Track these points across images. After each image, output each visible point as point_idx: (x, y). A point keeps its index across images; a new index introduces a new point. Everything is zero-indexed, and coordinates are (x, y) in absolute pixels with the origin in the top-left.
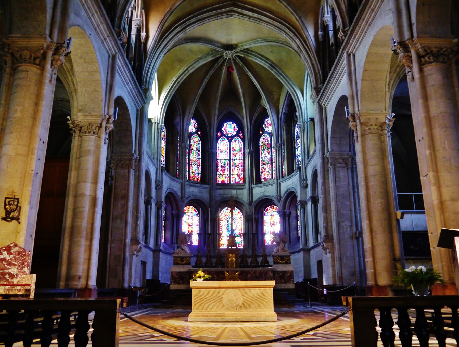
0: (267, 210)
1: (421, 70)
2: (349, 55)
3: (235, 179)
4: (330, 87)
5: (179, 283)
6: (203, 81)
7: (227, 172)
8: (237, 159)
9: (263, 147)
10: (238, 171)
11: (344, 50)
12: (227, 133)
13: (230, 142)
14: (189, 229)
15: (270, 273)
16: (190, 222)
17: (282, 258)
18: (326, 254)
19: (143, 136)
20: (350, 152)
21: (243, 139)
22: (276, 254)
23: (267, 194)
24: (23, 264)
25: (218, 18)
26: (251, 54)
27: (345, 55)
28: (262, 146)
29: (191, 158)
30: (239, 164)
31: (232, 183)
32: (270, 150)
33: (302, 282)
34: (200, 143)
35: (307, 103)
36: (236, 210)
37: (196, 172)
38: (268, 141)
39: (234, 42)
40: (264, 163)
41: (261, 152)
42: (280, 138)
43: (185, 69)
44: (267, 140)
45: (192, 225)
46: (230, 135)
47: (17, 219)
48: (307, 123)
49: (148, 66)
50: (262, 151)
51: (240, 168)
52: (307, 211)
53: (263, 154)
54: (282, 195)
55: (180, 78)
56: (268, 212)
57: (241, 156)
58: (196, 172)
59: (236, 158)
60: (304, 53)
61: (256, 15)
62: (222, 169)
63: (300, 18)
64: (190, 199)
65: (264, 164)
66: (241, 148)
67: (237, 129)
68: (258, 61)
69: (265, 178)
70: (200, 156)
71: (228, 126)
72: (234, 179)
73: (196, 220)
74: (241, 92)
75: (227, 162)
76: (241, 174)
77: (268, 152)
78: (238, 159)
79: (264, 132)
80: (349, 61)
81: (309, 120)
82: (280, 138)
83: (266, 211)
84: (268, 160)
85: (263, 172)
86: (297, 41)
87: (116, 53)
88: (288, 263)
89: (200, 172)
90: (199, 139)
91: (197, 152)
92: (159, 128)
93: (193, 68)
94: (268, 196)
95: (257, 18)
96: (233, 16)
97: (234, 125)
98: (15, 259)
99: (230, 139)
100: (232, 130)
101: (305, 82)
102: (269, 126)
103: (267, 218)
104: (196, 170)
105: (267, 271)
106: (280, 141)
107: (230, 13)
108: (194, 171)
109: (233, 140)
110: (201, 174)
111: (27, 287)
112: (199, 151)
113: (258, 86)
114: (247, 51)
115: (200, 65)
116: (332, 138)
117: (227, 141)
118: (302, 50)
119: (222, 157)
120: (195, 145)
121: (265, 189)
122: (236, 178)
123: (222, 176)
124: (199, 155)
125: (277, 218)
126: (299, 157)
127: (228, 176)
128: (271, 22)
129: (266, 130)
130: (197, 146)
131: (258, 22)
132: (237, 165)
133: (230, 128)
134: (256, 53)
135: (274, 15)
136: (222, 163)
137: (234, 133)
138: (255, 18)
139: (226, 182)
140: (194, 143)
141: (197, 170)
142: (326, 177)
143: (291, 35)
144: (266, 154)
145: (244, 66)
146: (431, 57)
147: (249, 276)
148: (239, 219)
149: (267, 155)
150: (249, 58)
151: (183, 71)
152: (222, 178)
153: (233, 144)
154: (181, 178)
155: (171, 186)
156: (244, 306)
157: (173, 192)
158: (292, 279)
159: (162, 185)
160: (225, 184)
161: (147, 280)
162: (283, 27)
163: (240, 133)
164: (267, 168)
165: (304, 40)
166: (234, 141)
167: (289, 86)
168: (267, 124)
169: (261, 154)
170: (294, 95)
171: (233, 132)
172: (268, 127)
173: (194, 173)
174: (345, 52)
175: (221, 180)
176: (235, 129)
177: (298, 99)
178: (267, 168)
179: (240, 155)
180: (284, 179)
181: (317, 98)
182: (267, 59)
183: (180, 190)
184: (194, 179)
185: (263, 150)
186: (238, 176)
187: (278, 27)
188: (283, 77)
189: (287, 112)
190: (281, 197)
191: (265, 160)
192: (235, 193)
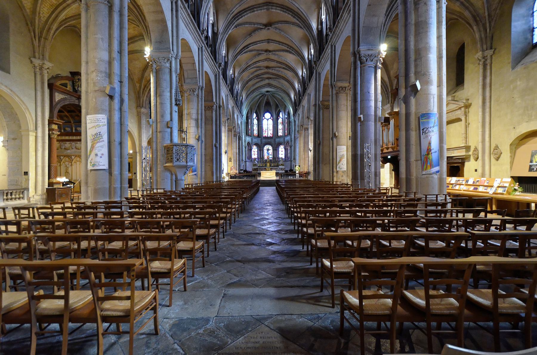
3: (270, 135)
21: (272, 120)
68: (277, 96)
73: (256, 150)
74: (272, 104)
78: (271, 127)
99: (268, 120)
103: (280, 149)
119: (265, 127)
125: (283, 150)
152: (265, 134)
156: (270, 175)
165: (291, 98)
178: (281, 131)
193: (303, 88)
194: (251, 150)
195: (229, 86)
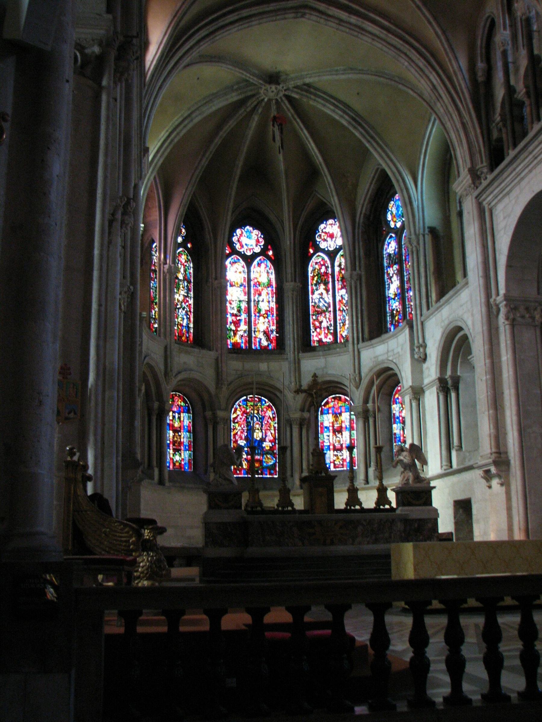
0: (327, 403)
4: (515, 169)
6: (211, 141)
7: (243, 327)
8: (263, 301)
9: (316, 279)
10: (266, 325)
12: (242, 246)
14: (175, 439)
15: (399, 524)
16: (177, 425)
18: (490, 487)
20: (539, 296)
23: (330, 372)
25: (278, 17)
26: (315, 95)
28: (313, 278)
29: (177, 296)
31: (253, 347)
32: (330, 286)
34: (192, 265)
35: (424, 198)
36: (264, 402)
37: (184, 324)
38: (327, 268)
39: (281, 68)
40: (318, 311)
41: (312, 290)
42: (357, 263)
43: (185, 115)
44: (324, 265)
46: (249, 253)
48: (424, 236)
50: (314, 288)
51: (270, 318)
52: (424, 407)
53: (316, 293)
54: (363, 375)
55: (175, 133)
56: (327, 406)
57: (270, 295)
58: (184, 324)
60: (446, 101)
61: (353, 19)
62: (235, 320)
63: (444, 32)
64: (180, 377)
65: (319, 313)
66: (270, 281)
68: (329, 110)
69: (320, 341)
70: (192, 293)
71: (244, 233)
72: (258, 340)
73: (186, 419)
75: (244, 305)
79: (317, 249)
81: (427, 231)
82: (357, 263)
83: (325, 405)
84: (326, 305)
85: (316, 329)
89: (191, 325)
90: (189, 258)
91: (186, 284)
93: (200, 114)
94: (333, 375)
95: (356, 26)
96: (307, 16)
97: (257, 233)
99: (249, 260)
100: (253, 242)
101: (422, 157)
102: (329, 239)
103: (327, 420)
104: (183, 319)
105: (393, 520)
106: (357, 269)
107: (302, 11)
109: (255, 262)
112: (189, 282)
113: (319, 159)
114: (308, 88)
115: (214, 108)
116: (509, 266)
117: (243, 263)
120: (182, 270)
122: (261, 339)
123: (235, 334)
124: (189, 290)
126: (392, 302)
127: (246, 335)
128: (382, 36)
129: (323, 245)
130: (185, 271)
131: (356, 34)
133: (249, 237)
134: (324, 93)
135: (390, 22)
136: (233, 308)
137: (257, 250)
138: (350, 24)
139: (243, 345)
141: (185, 321)
143: (421, 63)
144: (322, 294)
145: (296, 116)
147: (360, 528)
148: (270, 421)
150: (311, 102)
151: (181, 119)
153: (255, 270)
157: (153, 364)
160: (241, 348)
162: (406, 48)
163: (269, 250)
166: (256, 265)
167: (389, 162)
168: (323, 234)
169: (313, 293)
170: (398, 181)
171: (254, 246)
172: (325, 240)
173: (182, 325)
175: (233, 341)
176: (258, 241)
177: (407, 189)
179: (270, 292)
182: (346, 108)
183: (163, 360)
184: (181, 337)
185: (316, 285)
186: (266, 334)
187: (395, 47)
188: (378, 143)
189: (368, 213)
190: (360, 379)
191: (321, 305)
194: (162, 414)
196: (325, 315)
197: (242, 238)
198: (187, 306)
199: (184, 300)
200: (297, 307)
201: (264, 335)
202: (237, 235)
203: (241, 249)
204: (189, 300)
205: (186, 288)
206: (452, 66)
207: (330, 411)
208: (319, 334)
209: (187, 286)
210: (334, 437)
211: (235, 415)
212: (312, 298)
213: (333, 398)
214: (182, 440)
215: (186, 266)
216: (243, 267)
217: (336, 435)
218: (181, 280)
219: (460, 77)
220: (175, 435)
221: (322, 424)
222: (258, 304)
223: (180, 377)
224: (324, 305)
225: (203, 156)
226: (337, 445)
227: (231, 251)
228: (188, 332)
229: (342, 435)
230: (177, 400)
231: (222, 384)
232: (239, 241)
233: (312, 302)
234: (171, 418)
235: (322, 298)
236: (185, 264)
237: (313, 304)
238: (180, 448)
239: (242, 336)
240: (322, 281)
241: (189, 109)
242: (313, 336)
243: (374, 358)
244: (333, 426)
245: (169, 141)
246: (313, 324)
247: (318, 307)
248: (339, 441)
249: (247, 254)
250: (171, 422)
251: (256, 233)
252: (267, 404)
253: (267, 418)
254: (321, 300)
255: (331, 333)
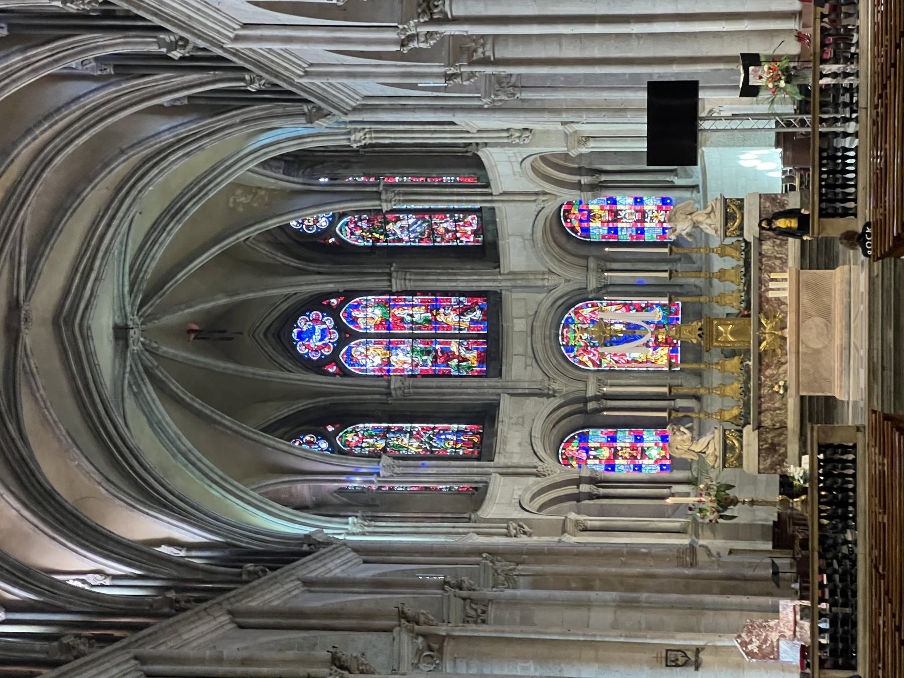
0: (573, 229)
1: (456, 20)
2: (307, 74)
5: (785, 455)
6: (198, 414)
7: (454, 347)
11: (292, 84)
12: (326, 345)
13: (356, 336)
14: (627, 455)
16: (605, 453)
17: (728, 218)
19: (432, 548)
21: (348, 295)
22: (721, 232)
24: (765, 626)
27: (304, 81)
29: (413, 450)
30: (426, 307)
33: (785, 151)
34: (361, 426)
37: (455, 438)
38: (361, 220)
41: (394, 241)
42: (368, 189)
45: (615, 448)
46: (336, 336)
47: (698, 650)
49: (246, 540)
50: (392, 237)
55: (211, 474)
56: (578, 229)
58: (455, 438)
59: (408, 318)
62: (442, 359)
63: (122, 152)
65: (432, 231)
66: (378, 304)
67: (313, 315)
68: (159, 252)
69: (475, 233)
74: (224, 301)
75: (419, 346)
76: (460, 302)
77: (395, 222)
79: (329, 231)
80: (319, 75)
83: (576, 233)
84: (419, 222)
85: (457, 238)
86: (172, 158)
87: (298, 579)
88: (740, 204)
89: (455, 427)
90: (349, 429)
92: (360, 530)
98: (757, 636)
99: (347, 335)
100: (319, 328)
104: (447, 439)
108: (452, 443)
110: (459, 423)
111: (798, 609)
113: (215, 250)
118: (197, 146)
120: (371, 441)
121: (513, 235)
122: (472, 320)
123: (465, 360)
124: (400, 430)
127: (465, 343)
130: (371, 436)
132: (429, 314)
135: (102, 217)
137: (329, 322)
140: (364, 445)
141: (449, 437)
142: (538, 105)
143: (155, 171)
145: (160, 294)
146: (436, 3)
149: (404, 223)
150: (148, 276)
154: (484, 478)
155: (513, 501)
156: (826, 314)
157: (528, 496)
158: (779, 197)
159: (521, 520)
160: (485, 351)
161: (774, 547)
162: (134, 192)
164: (445, 225)
165: (180, 143)
168: (306, 223)
169: (400, 240)
173: (456, 442)
174: (297, 80)
176: (316, 321)
178: (444, 224)
180: (492, 184)
181: (334, 115)
185: (387, 236)
186: (462, 312)
191: (419, 230)
192: (523, 321)
193: (100, 38)
195: (69, 648)
196: (436, 224)
197: (312, 346)
198: (425, 433)
199: (418, 438)
200: (428, 274)
201: (464, 316)
202: (307, 354)
203: (329, 348)
204: (417, 430)
205: (397, 435)
206: (168, 138)
207: (585, 225)
208: (465, 234)
209: (394, 433)
210: (624, 220)
211: (590, 364)
212: (407, 242)
213: (566, 221)
214: (628, 445)
215: (363, 435)
216: (358, 345)
217: (622, 219)
218: (387, 444)
219: (182, 130)
220: (621, 456)
221: (603, 237)
222: (417, 323)
223: (541, 452)
224: (420, 226)
225: (219, 423)
226: (638, 216)
227: (333, 363)
228: (464, 432)
229: (621, 210)
230: (570, 453)
231: (549, 389)
232: (316, 351)
233: (414, 242)
234: (597, 461)
235: (408, 229)
236: (360, 436)
237: (417, 240)
238: (639, 449)
239: (467, 349)
240: (381, 227)
241: (174, 456)
242: (467, 242)
243: (515, 174)
244: (608, 222)
245: (224, 483)
246: (449, 242)
247: (422, 234)
248: (631, 213)
249: (336, 339)
250: (603, 462)
251: (303, 324)
252: (573, 315)
253: (593, 316)
254: (411, 229)
255: (464, 218)
